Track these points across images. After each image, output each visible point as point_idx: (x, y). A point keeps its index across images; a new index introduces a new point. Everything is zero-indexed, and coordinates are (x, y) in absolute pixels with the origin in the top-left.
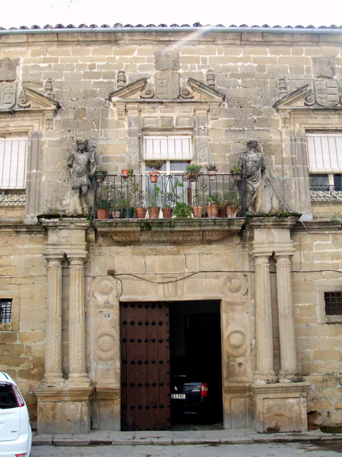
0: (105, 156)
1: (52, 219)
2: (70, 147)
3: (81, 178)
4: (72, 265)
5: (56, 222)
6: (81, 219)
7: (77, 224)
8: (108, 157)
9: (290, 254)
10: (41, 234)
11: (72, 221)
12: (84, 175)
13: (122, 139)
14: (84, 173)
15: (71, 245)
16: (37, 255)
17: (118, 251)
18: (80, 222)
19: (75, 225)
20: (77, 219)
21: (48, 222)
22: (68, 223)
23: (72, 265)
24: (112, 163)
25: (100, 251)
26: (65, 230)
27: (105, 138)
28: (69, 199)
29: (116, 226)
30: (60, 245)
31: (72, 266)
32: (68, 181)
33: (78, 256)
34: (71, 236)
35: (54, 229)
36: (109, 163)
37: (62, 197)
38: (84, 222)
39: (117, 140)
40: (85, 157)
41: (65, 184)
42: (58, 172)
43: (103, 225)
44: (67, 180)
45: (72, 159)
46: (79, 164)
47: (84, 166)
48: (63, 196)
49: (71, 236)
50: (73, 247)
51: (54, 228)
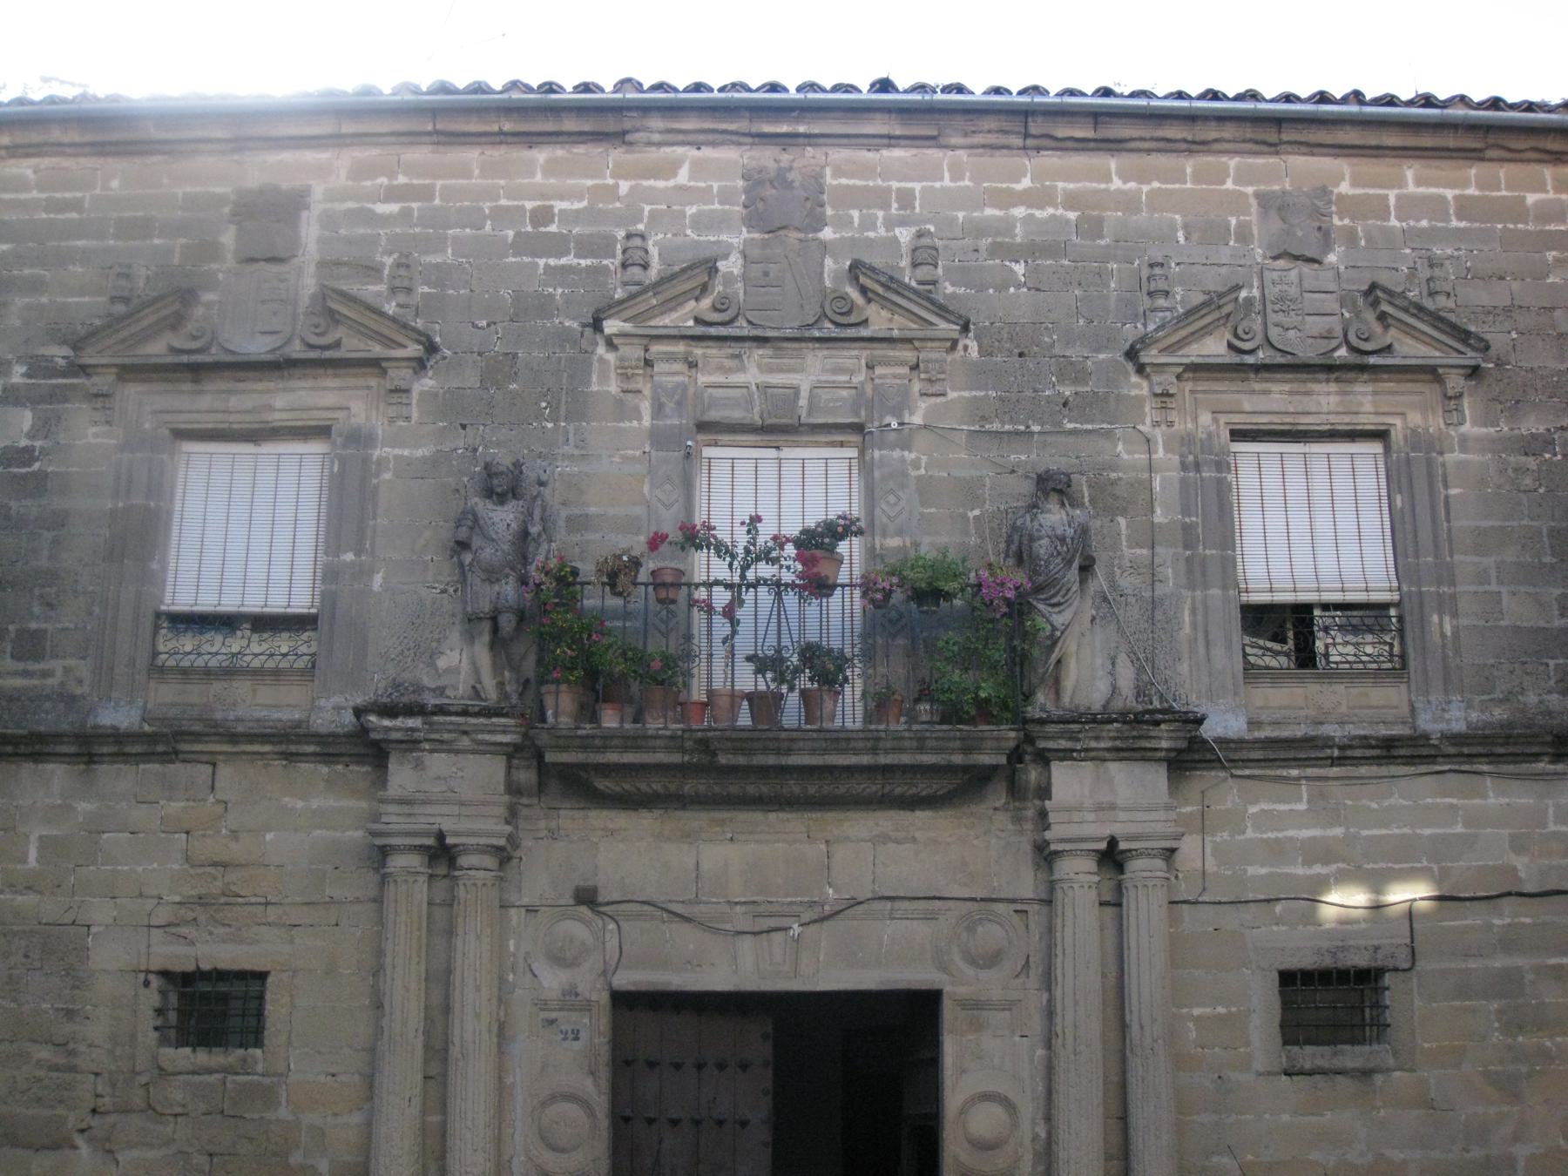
0: (577, 511)
1: (400, 719)
2: (466, 479)
3: (497, 587)
4: (462, 868)
5: (413, 730)
6: (494, 720)
7: (480, 737)
8: (587, 515)
9: (1168, 844)
10: (363, 763)
11: (465, 728)
12: (507, 576)
13: (634, 458)
14: (507, 570)
15: (462, 804)
16: (350, 833)
17: (611, 826)
18: (490, 732)
19: (473, 741)
20: (482, 720)
21: (388, 729)
22: (450, 731)
23: (462, 868)
24: (598, 536)
25: (553, 824)
26: (443, 755)
27: (577, 452)
28: (458, 651)
29: (605, 747)
30: (424, 803)
31: (460, 873)
32: (455, 591)
33: (483, 841)
34: (460, 774)
35: (406, 751)
36: (589, 536)
37: (434, 645)
38: (504, 732)
39: (617, 459)
40: (511, 516)
41: (445, 602)
42: (424, 562)
43: (561, 742)
44: (451, 590)
45: (470, 523)
46: (493, 540)
47: (506, 547)
48: (438, 641)
49: (460, 774)
50: (465, 811)
51: (404, 746)
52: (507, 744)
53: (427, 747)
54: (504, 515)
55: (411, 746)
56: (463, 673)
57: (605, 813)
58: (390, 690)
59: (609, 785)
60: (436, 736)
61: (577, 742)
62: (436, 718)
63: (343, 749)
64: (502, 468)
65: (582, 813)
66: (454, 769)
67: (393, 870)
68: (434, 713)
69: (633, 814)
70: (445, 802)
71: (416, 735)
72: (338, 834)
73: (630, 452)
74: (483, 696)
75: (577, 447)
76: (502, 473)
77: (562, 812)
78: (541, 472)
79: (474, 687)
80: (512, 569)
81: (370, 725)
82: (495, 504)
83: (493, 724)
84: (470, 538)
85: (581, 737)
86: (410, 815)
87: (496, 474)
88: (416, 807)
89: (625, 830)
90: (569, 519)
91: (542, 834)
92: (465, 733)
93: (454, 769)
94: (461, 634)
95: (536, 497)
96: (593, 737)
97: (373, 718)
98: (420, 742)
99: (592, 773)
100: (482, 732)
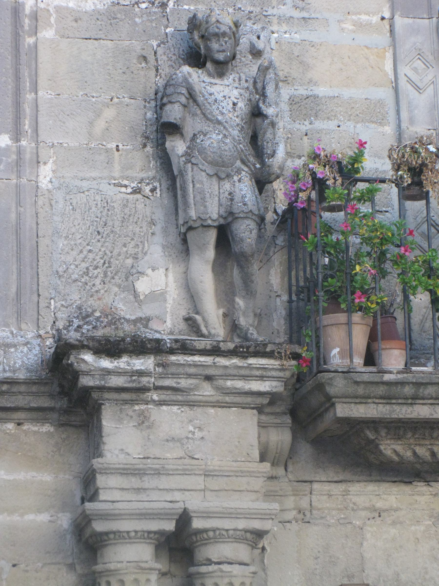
0: (302, 91)
1: (125, 359)
2: (155, 43)
3: (227, 186)
4: (209, 562)
5: (141, 373)
6: (252, 361)
7: (229, 383)
8: (316, 97)
9: (257, 525)
10: (43, 421)
11: (211, 372)
12: (239, 172)
13: (369, 24)
14: (238, 163)
15: (207, 474)
16: (30, 517)
17: (379, 505)
18: (244, 377)
19: (218, 388)
20: (235, 361)
21: (108, 372)
22: (190, 376)
23: (209, 562)
24: (332, 125)
25: (304, 503)
26: (175, 408)
27: (297, 14)
28: (162, 271)
29: (415, 397)
30: (158, 473)
31: (211, 568)
32: (153, 190)
33: (242, 524)
34: (198, 434)
35: (126, 402)
36: (319, 125)
37: (129, 261)
38: (262, 378)
39: (348, 26)
40: (236, 92)
41: (140, 206)
42: (107, 151)
43: (361, 390)
44: (147, 189)
45: (183, 100)
46: (219, 123)
47: (235, 133)
48: (136, 258)
49: (198, 434)
50: (214, 484)
51: (125, 396)
52: (260, 394)
53: (155, 397)
54: (227, 91)
55: (133, 396)
56: (170, 301)
57: (371, 487)
58: (76, 323)
59: (399, 448)
60: (167, 383)
61: (381, 390)
62: (173, 358)
63: (21, 401)
64: (224, 28)
65: (342, 487)
66: (191, 428)
67: (119, 565)
68: (172, 352)
69: (407, 489)
70: (186, 472)
71: (145, 380)
72: (16, 518)
73: (364, 18)
74: (204, 330)
75: (296, 7)
76: (224, 34)
77: (316, 486)
78: (255, 38)
79: (188, 320)
80: (243, 162)
81: (83, 367)
82: (210, 75)
83: (250, 368)
84: (183, 119)
85: (388, 384)
86: (138, 490)
87: (216, 35)
88: (146, 478)
89: (396, 510)
90: (292, 101)
91: (290, 515)
92: (208, 378)
93: (191, 428)
94: (164, 247)
95: (267, 68)
96: (402, 383)
97: (88, 357)
98: (148, 390)
99: (383, 433)
100: (233, 377)
